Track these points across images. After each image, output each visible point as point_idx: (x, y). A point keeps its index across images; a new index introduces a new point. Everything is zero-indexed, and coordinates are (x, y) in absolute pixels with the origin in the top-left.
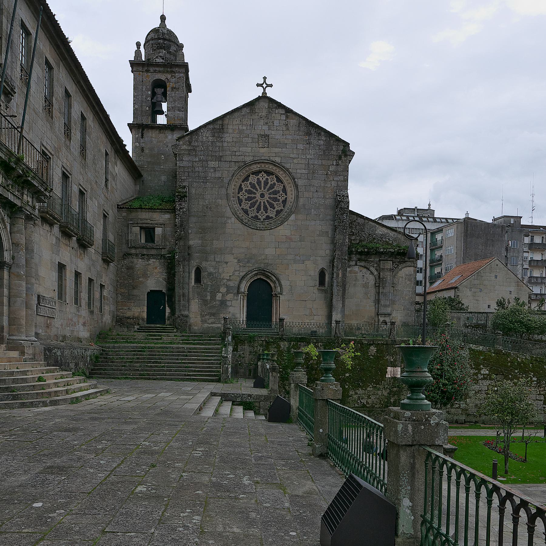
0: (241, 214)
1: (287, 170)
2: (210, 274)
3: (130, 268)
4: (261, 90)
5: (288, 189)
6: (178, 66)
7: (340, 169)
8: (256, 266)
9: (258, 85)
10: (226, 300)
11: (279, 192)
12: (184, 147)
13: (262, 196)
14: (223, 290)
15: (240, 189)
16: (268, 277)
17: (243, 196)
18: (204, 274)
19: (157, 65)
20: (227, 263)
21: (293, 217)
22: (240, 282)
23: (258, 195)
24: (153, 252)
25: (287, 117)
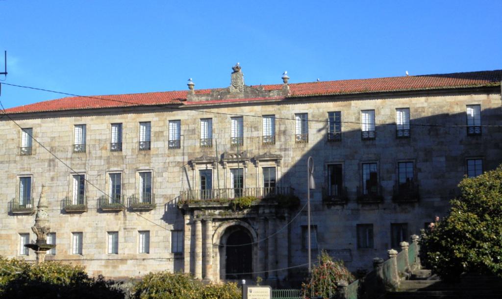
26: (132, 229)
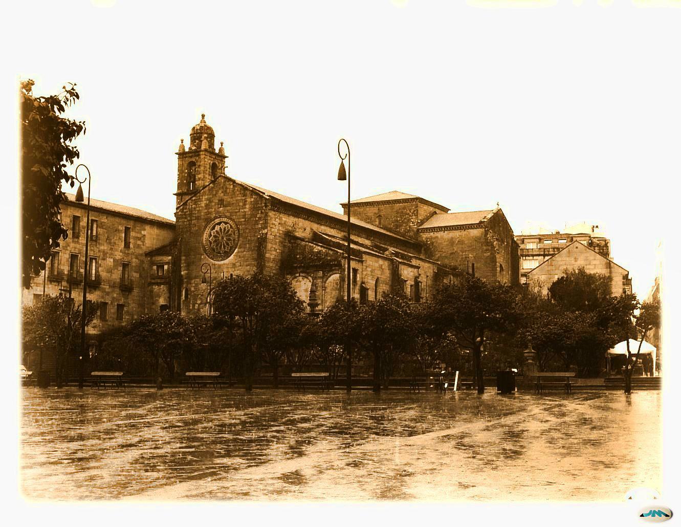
3: (152, 291)
15: (210, 235)
25: (234, 186)
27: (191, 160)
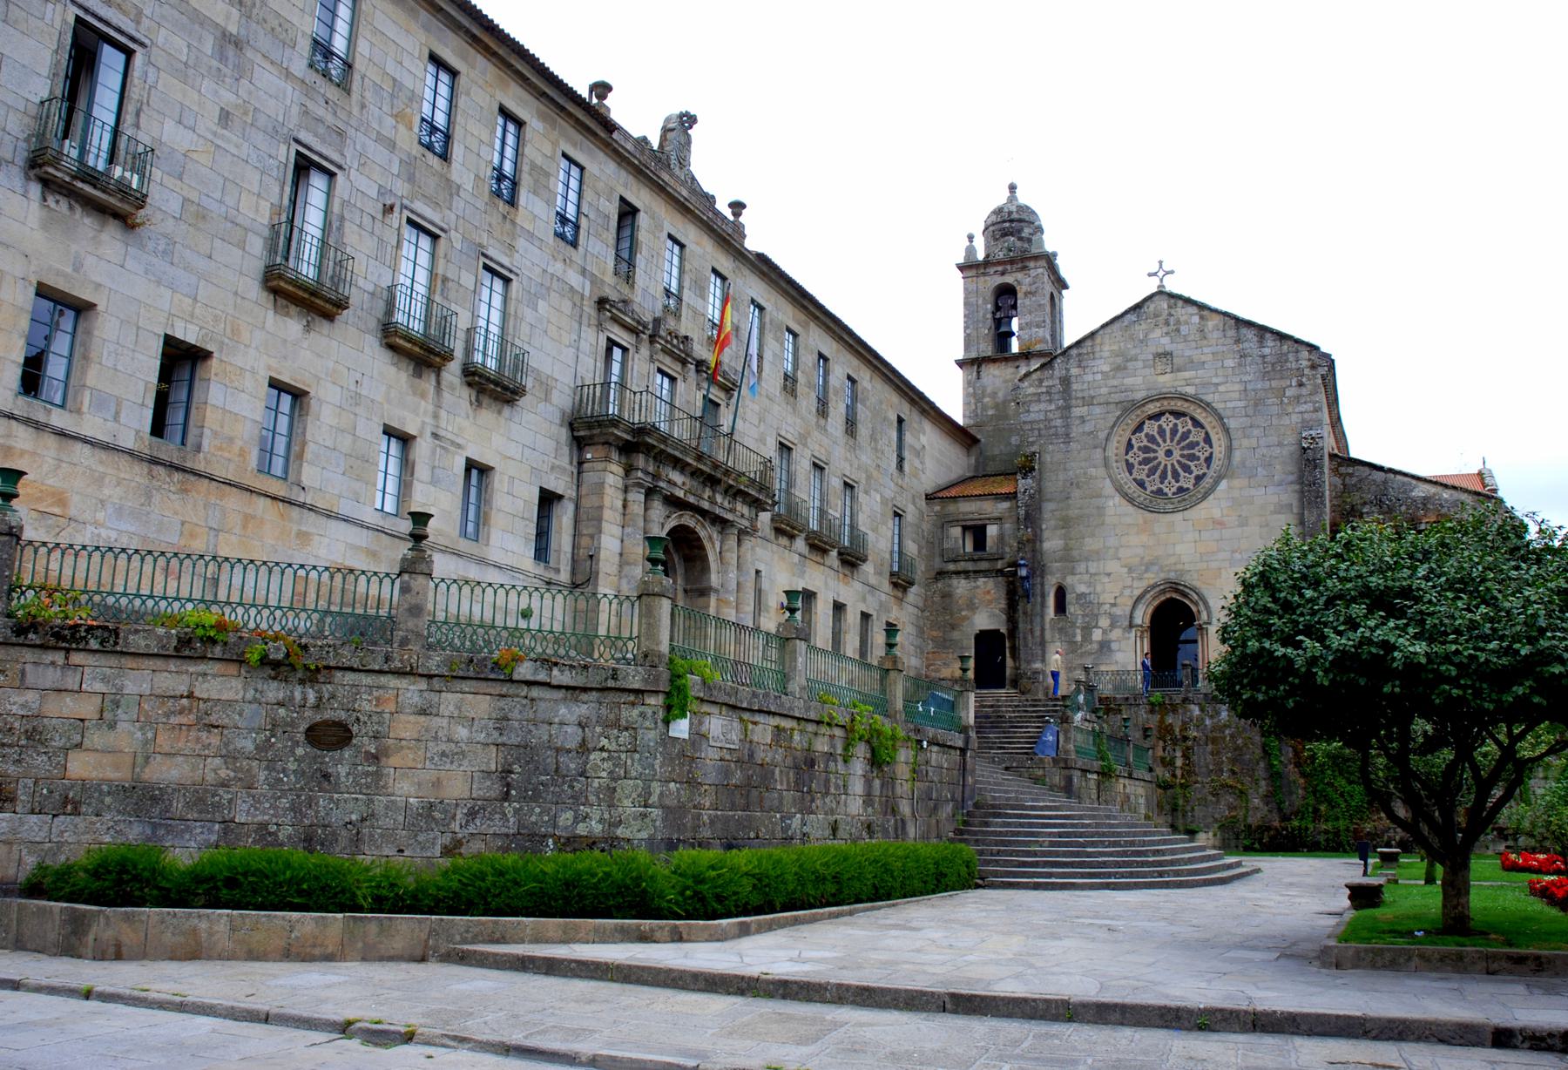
0: (1133, 488)
1: (1208, 404)
2: (1083, 595)
3: (946, 595)
4: (1155, 282)
5: (1214, 438)
6: (1036, 258)
7: (1304, 391)
8: (1163, 576)
9: (1150, 275)
10: (1110, 642)
11: (1198, 444)
12: (1031, 390)
13: (1169, 453)
14: (1104, 622)
15: (1130, 446)
16: (1185, 595)
17: (1135, 457)
18: (1069, 597)
19: (999, 263)
20: (1109, 575)
21: (1224, 484)
22: (1134, 607)
23: (1161, 454)
24: (984, 565)
25: (1202, 317)
26: (453, 443)
27: (999, 280)
